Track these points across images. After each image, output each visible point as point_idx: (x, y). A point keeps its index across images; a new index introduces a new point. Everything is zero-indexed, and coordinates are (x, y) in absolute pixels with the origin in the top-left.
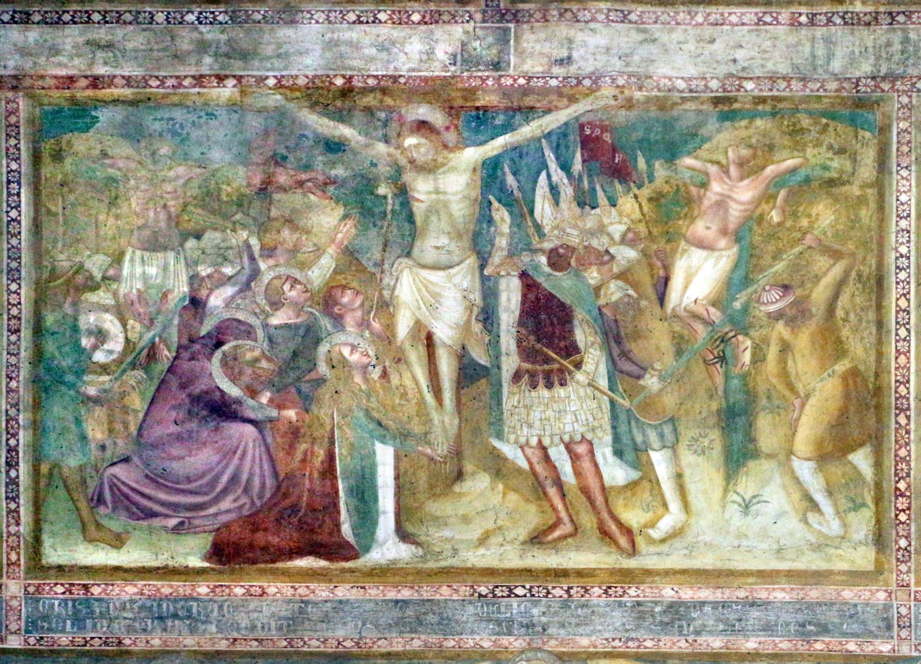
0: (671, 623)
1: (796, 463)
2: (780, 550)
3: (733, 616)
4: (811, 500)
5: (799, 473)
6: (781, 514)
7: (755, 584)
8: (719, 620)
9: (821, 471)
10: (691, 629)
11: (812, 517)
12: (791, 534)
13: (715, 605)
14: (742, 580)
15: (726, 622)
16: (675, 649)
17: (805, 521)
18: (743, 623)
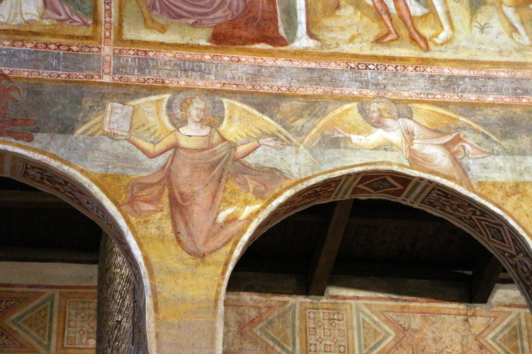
0: (449, 86)
1: (505, 8)
2: (500, 52)
3: (480, 84)
4: (514, 27)
5: (507, 13)
6: (500, 33)
7: (490, 68)
8: (473, 86)
9: (517, 12)
10: (460, 90)
11: (514, 34)
12: (505, 43)
13: (471, 78)
14: (483, 66)
15: (477, 87)
16: (452, 100)
17: (511, 37)
18: (485, 88)
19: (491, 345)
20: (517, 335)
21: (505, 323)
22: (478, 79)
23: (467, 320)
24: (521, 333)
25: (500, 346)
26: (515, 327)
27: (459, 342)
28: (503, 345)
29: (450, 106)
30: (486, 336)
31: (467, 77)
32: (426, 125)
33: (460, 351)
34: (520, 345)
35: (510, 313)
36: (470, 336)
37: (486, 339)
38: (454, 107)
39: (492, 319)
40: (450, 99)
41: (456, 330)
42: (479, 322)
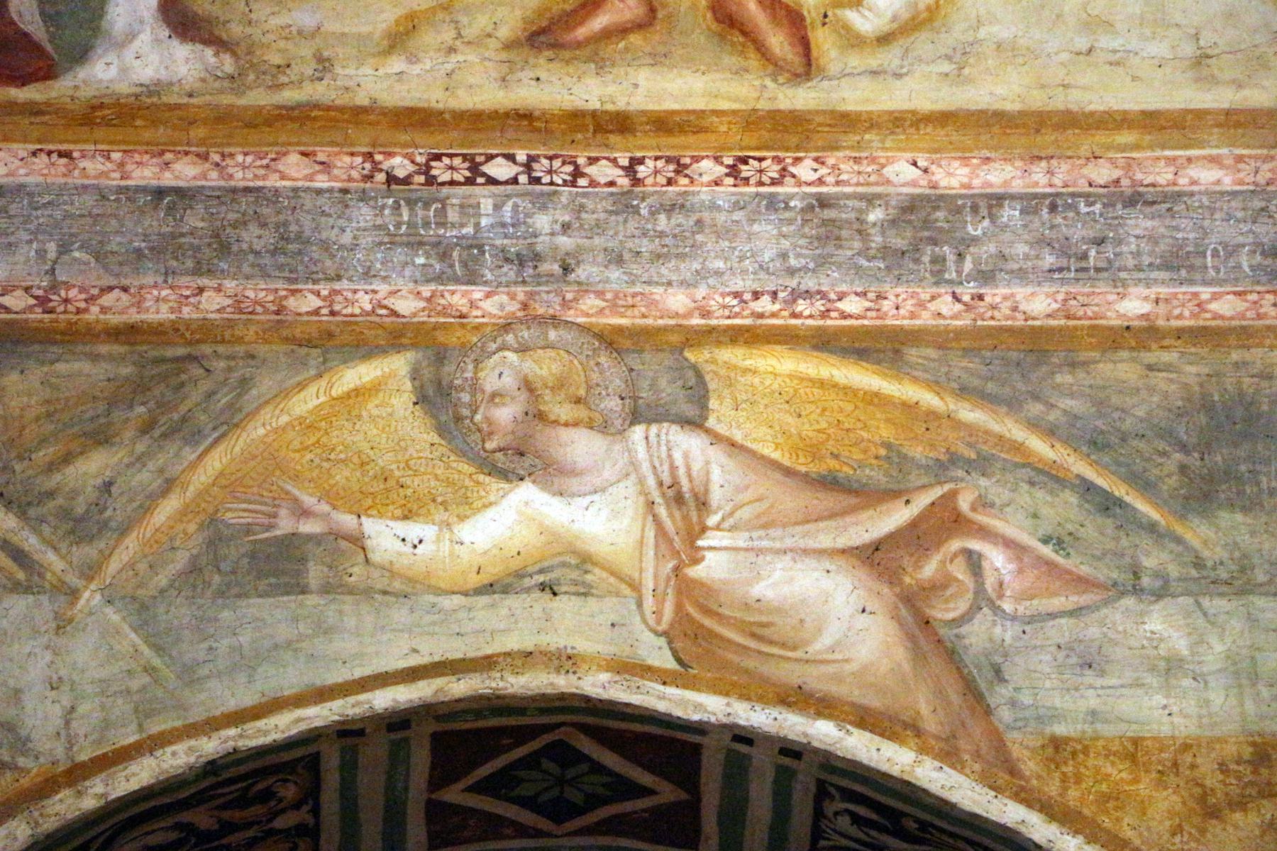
2: (1201, 60)
3: (1078, 233)
7: (1137, 147)
8: (1043, 242)
10: (968, 265)
13: (1031, 203)
14: (1101, 138)
15: (1064, 248)
16: (925, 319)
22: (1073, 207)
29: (912, 354)
31: (1013, 197)
32: (776, 455)
38: (932, 353)
40: (913, 316)
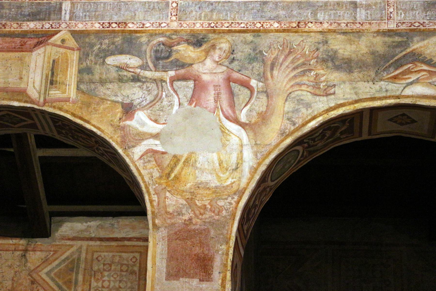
19: (44, 280)
20: (73, 268)
21: (63, 257)
23: (25, 255)
24: (78, 267)
25: (53, 279)
26: (74, 260)
27: (11, 279)
28: (57, 279)
30: (40, 271)
33: (9, 287)
34: (74, 278)
35: (72, 246)
36: (24, 272)
37: (40, 274)
39: (52, 253)
41: (10, 267)
42: (35, 257)
